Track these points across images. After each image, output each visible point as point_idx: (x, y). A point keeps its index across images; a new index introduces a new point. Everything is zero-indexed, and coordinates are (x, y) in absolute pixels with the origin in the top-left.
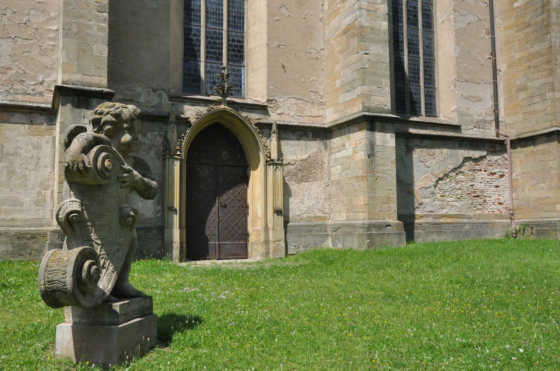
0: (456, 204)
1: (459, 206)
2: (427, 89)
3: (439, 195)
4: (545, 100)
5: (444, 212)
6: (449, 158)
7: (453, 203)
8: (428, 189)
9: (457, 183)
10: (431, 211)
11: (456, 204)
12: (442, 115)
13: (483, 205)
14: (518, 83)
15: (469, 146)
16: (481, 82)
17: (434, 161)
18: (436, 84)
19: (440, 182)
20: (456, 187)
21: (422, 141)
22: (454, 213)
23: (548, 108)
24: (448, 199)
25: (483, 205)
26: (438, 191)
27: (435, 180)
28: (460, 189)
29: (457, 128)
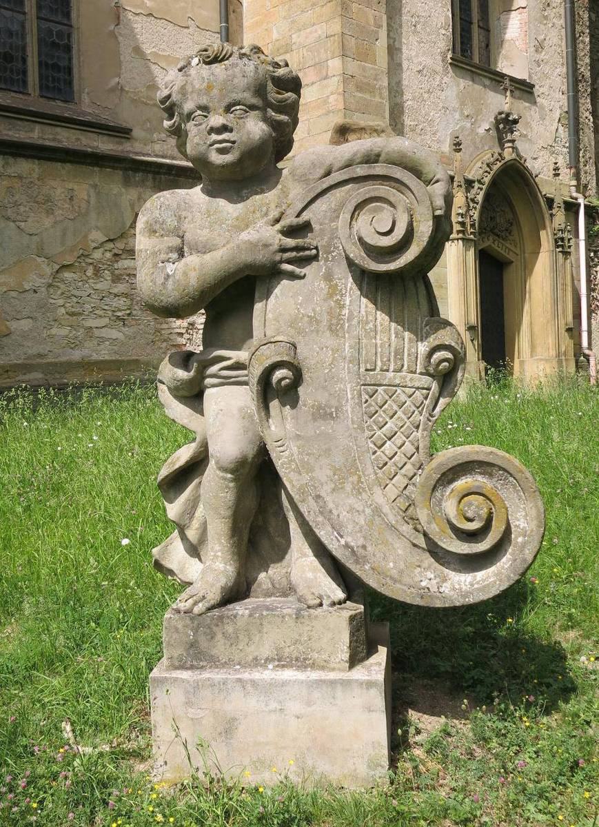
0: (114, 334)
1: (120, 336)
2: (45, 25)
3: (63, 310)
4: (326, 78)
5: (76, 355)
6: (93, 215)
7: (105, 333)
8: (30, 295)
9: (117, 279)
10: (40, 356)
11: (114, 334)
12: (86, 99)
13: (186, 336)
14: (275, 36)
15: (149, 183)
16: (190, 22)
17: (48, 222)
18: (74, 15)
19: (67, 275)
20: (115, 291)
21: (11, 160)
22: (107, 358)
23: (332, 99)
24: (91, 323)
25: (186, 336)
26: (61, 302)
27: (48, 271)
28: (126, 295)
29: (123, 133)
